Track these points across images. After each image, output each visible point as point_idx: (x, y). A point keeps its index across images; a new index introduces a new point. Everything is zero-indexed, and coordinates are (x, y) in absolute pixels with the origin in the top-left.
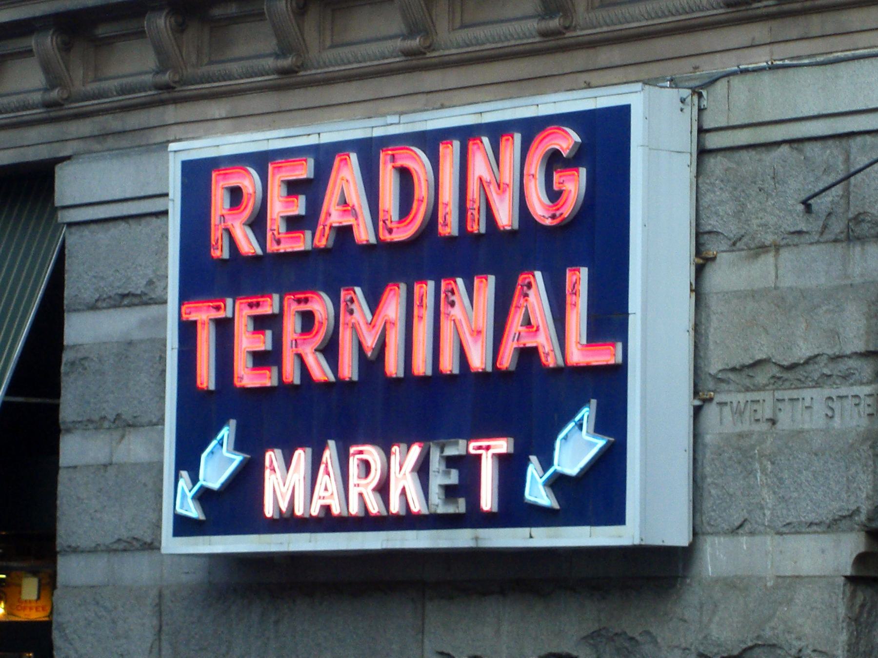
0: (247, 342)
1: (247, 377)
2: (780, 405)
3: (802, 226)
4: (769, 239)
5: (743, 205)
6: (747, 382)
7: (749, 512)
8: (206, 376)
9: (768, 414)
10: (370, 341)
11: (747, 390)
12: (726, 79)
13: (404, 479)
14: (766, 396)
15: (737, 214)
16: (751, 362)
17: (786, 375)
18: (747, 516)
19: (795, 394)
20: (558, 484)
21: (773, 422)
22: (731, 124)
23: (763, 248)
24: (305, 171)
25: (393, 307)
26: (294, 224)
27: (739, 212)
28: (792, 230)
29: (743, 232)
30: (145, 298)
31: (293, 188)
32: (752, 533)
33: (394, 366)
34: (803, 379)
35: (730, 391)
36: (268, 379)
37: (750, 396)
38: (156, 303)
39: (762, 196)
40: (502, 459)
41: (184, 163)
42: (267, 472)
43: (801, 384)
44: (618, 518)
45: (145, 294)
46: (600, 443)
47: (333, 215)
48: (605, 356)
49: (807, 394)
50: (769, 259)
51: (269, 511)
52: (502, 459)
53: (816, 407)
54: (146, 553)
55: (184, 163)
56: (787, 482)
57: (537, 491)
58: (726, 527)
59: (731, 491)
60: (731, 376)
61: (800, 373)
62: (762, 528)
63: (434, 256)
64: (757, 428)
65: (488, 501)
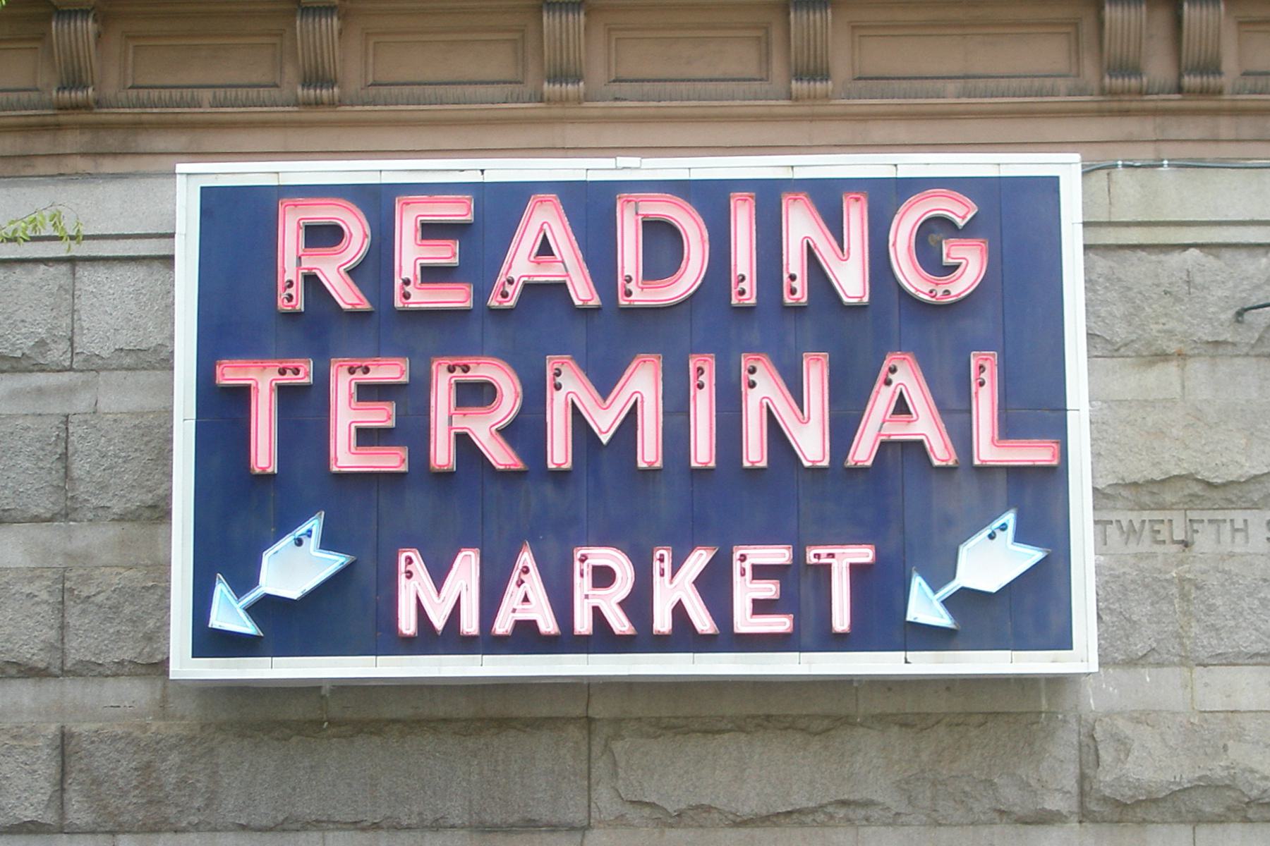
0: (346, 416)
1: (346, 456)
2: (1196, 526)
3: (1227, 336)
4: (1173, 347)
5: (1139, 308)
6: (1146, 499)
7: (1158, 642)
8: (264, 454)
9: (1179, 535)
10: (604, 422)
11: (1143, 508)
12: (1106, 171)
13: (676, 589)
14: (1178, 517)
15: (1128, 319)
16: (1163, 477)
17: (1208, 494)
18: (1154, 645)
19: (1219, 515)
20: (964, 601)
21: (1186, 544)
22: (1113, 219)
23: (1163, 357)
24: (457, 211)
25: (642, 383)
26: (431, 274)
27: (1131, 314)
28: (1210, 340)
29: (1134, 337)
30: (25, 363)
31: (430, 231)
32: (1159, 665)
33: (649, 452)
34: (1234, 499)
35: (1115, 508)
36: (391, 460)
37: (1147, 515)
38: (43, 371)
39: (1167, 300)
40: (855, 569)
41: (205, 191)
42: (402, 578)
43: (1230, 504)
44: (1064, 642)
45: (29, 358)
46: (1031, 556)
47: (520, 265)
48: (1036, 454)
49: (1239, 516)
50: (1172, 368)
51: (407, 624)
52: (856, 570)
53: (1251, 531)
54: (30, 681)
55: (205, 191)
56: (1221, 609)
57: (924, 606)
58: (1120, 658)
59: (1135, 618)
60: (1125, 493)
61: (1232, 493)
62: (1176, 659)
63: (716, 326)
64: (1159, 549)
65: (841, 620)
